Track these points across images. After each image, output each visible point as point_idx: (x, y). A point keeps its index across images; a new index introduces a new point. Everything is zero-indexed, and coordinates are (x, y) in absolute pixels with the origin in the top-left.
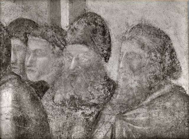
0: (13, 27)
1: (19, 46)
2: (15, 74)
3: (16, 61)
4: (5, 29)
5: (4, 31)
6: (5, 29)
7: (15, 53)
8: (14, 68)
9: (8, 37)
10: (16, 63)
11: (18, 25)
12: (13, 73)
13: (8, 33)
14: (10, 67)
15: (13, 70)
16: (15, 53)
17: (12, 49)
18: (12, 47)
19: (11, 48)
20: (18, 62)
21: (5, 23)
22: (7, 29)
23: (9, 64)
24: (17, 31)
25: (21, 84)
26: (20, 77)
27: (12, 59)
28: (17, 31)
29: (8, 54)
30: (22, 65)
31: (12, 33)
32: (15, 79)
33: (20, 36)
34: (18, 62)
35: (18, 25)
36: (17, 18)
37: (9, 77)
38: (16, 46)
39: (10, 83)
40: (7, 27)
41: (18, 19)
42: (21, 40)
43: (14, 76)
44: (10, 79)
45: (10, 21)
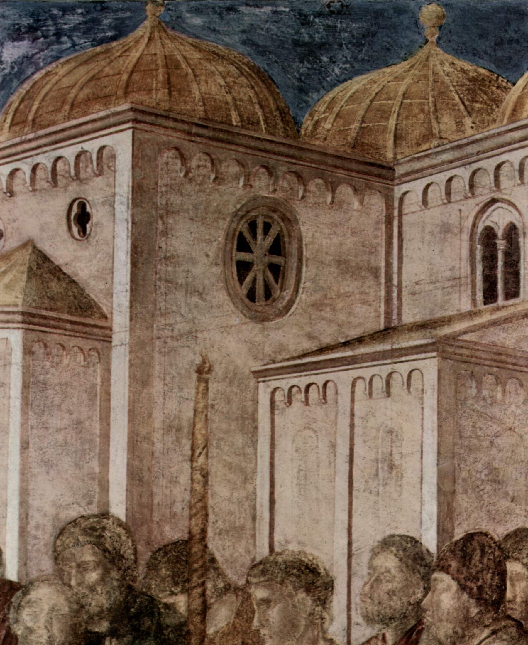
0: (509, 543)
1: (519, 573)
2: (513, 619)
3: (515, 597)
4: (496, 546)
5: (494, 549)
6: (496, 546)
7: (513, 585)
8: (512, 609)
9: (502, 558)
10: (514, 601)
11: (517, 539)
12: (509, 617)
13: (502, 552)
14: (504, 607)
15: (509, 612)
16: (513, 585)
17: (508, 577)
18: (509, 574)
19: (506, 577)
20: (519, 600)
21: (498, 535)
22: (500, 545)
23: (503, 602)
24: (516, 549)
25: (522, 635)
26: (521, 625)
27: (509, 595)
28: (516, 549)
29: (501, 586)
30: (524, 605)
31: (509, 553)
32: (513, 627)
33: (521, 556)
34: (519, 600)
35: (517, 539)
36: (517, 527)
37: (503, 623)
38: (514, 573)
39: (505, 633)
40: (499, 541)
41: (518, 529)
42: (523, 564)
43: (510, 622)
44: (505, 627)
45: (506, 533)
